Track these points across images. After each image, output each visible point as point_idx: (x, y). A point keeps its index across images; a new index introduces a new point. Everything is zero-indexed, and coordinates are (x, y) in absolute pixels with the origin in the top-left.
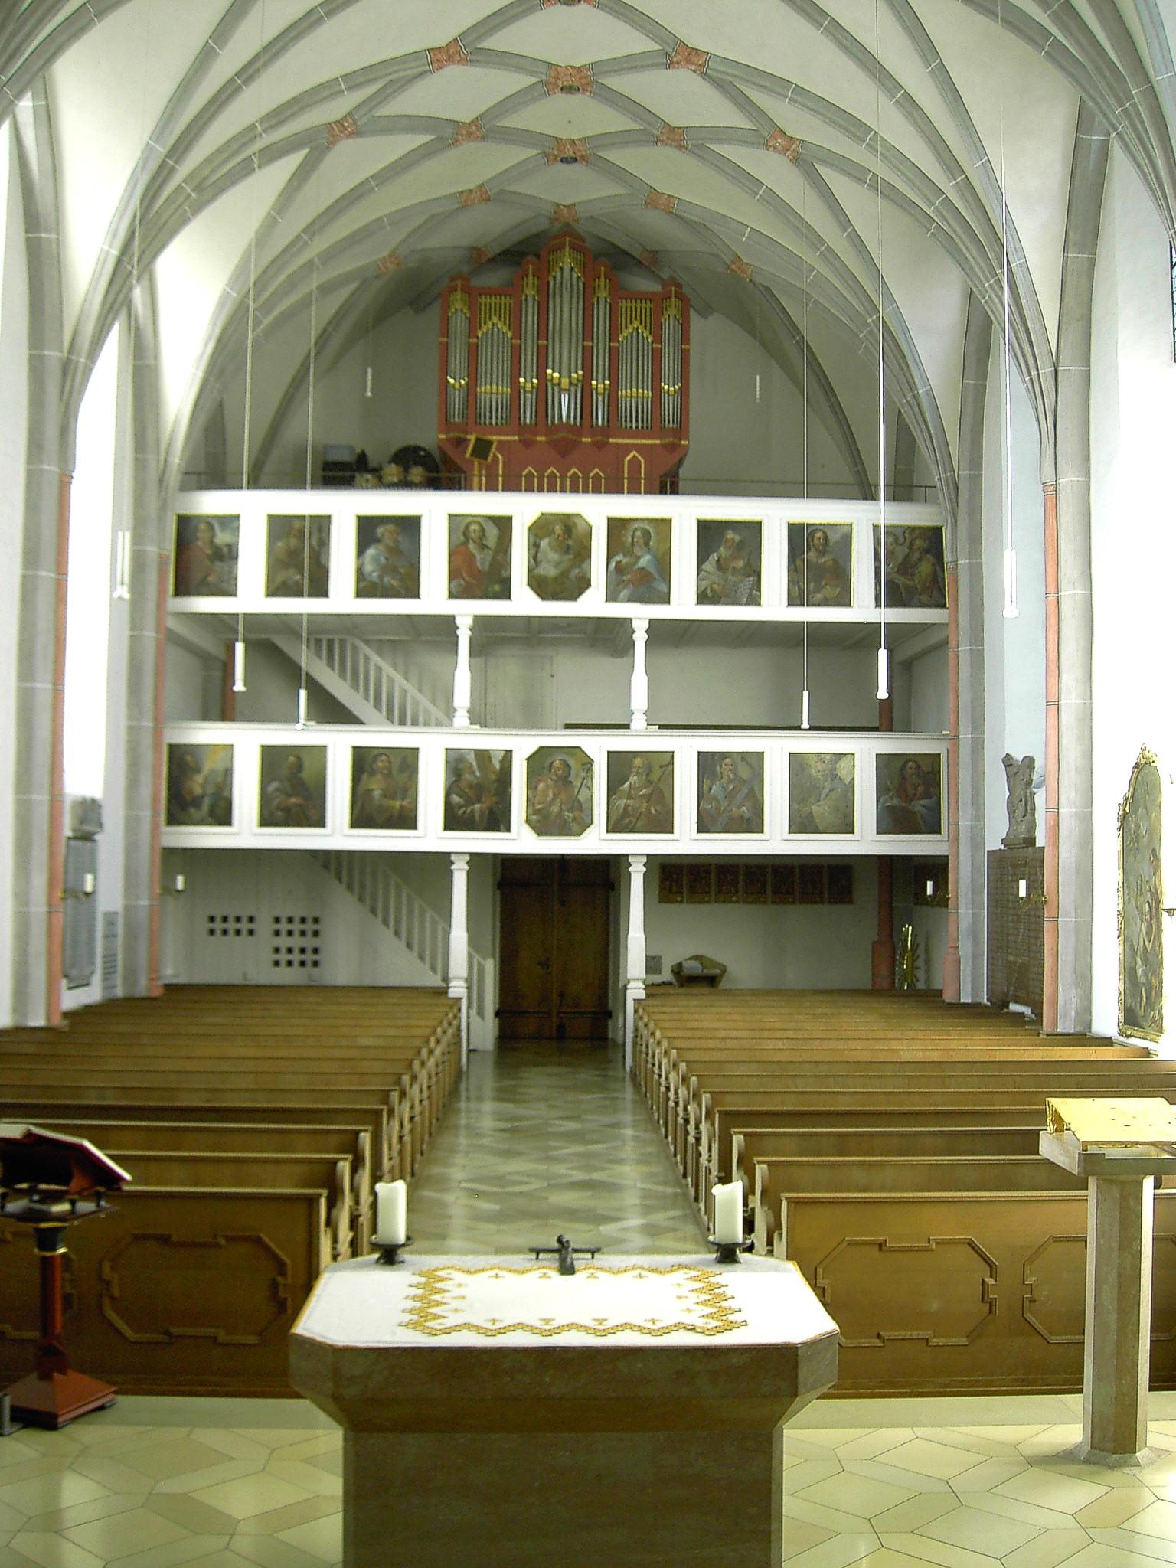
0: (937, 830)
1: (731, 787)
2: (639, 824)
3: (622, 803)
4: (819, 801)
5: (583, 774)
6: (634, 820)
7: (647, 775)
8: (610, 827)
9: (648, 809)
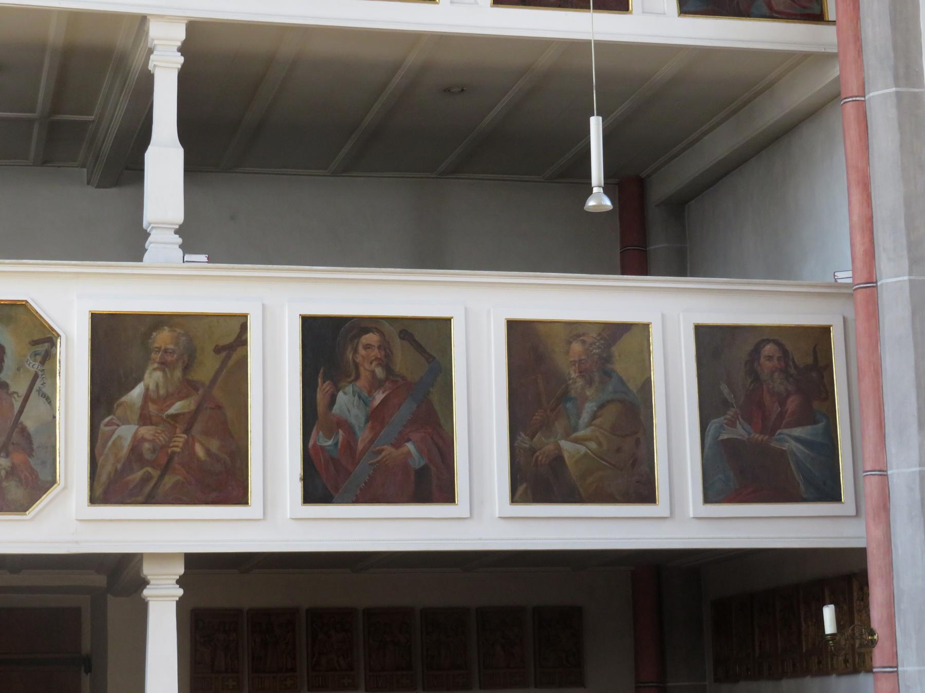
0: (832, 494)
1: (379, 397)
2: (169, 481)
3: (126, 433)
4: (575, 429)
5: (33, 366)
6: (156, 473)
7: (186, 369)
8: (99, 492)
9: (189, 446)
